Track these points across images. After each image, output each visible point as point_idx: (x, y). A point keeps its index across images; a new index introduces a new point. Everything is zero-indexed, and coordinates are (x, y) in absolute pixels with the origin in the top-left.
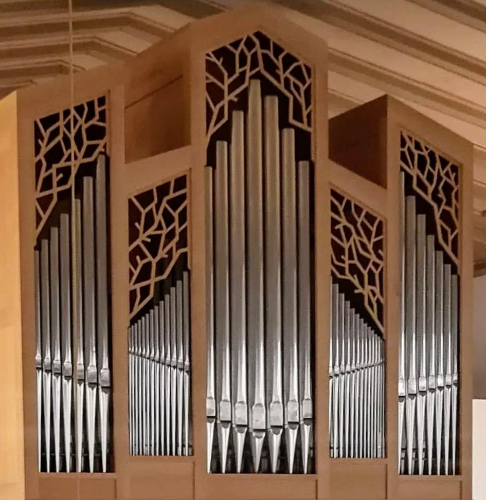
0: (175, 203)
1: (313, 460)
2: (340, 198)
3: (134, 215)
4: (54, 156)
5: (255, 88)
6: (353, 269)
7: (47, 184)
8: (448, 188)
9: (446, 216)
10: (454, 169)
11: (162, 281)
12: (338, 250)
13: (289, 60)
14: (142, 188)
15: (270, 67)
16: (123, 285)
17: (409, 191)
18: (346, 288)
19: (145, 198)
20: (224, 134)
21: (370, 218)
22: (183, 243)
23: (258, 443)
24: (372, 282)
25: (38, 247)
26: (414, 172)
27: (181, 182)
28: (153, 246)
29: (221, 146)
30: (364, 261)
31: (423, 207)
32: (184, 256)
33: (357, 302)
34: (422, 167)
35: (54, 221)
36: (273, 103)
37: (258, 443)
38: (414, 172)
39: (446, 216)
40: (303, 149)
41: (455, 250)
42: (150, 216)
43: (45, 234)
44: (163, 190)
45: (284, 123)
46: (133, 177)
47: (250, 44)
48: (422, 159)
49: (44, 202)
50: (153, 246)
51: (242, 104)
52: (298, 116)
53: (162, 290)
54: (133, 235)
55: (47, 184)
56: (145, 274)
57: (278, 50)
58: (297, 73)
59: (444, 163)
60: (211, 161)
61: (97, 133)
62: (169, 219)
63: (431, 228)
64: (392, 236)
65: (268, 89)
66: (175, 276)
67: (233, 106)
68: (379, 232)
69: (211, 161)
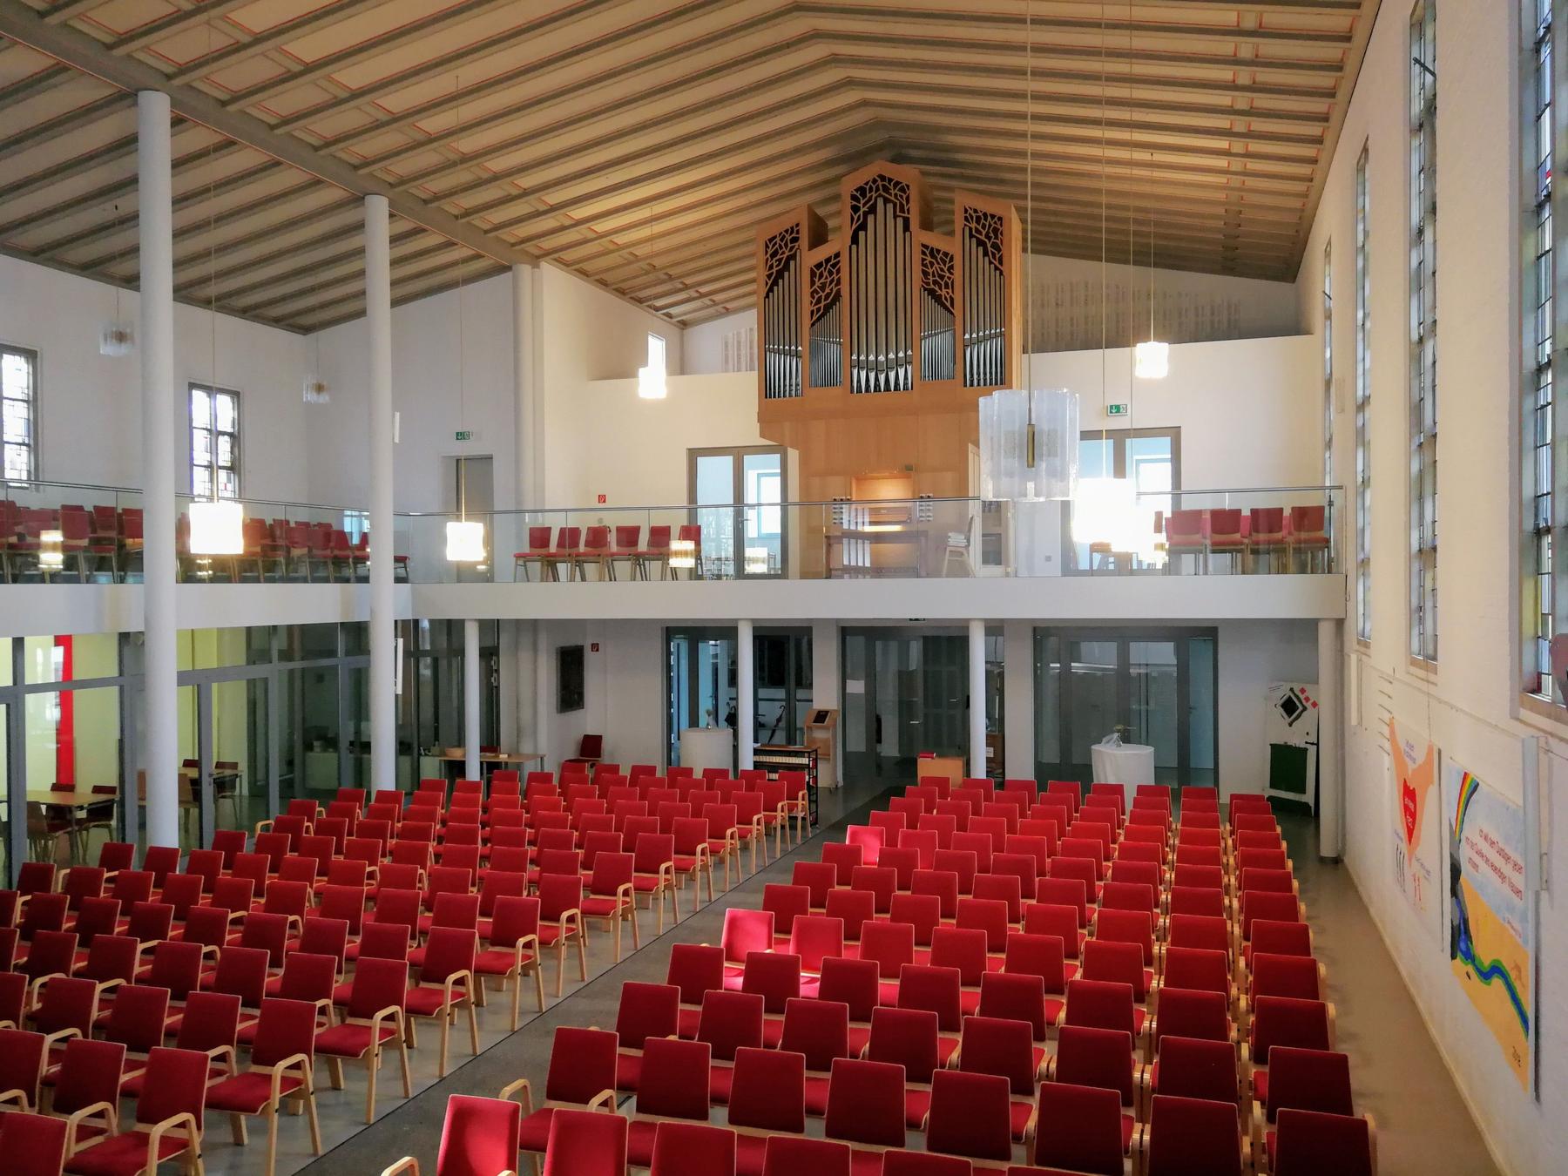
0: (834, 266)
1: (905, 384)
2: (926, 247)
3: (813, 274)
4: (774, 255)
5: (880, 202)
6: (935, 282)
7: (771, 267)
8: (996, 231)
9: (995, 246)
10: (1000, 219)
11: (826, 306)
12: (925, 274)
13: (897, 183)
14: (816, 261)
15: (886, 189)
16: (807, 305)
17: (971, 236)
18: (932, 293)
19: (819, 266)
20: (863, 227)
21: (946, 254)
22: (838, 283)
23: (882, 378)
24: (947, 286)
25: (767, 296)
26: (973, 225)
27: (837, 255)
28: (823, 288)
29: (862, 234)
30: (942, 277)
31: (980, 243)
32: (838, 292)
33: (937, 299)
34: (978, 221)
35: (775, 283)
36: (890, 206)
37: (882, 378)
38: (973, 225)
39: (995, 246)
40: (906, 228)
41: (1001, 262)
42: (821, 276)
43: (771, 290)
44: (828, 260)
45: (895, 217)
46: (810, 258)
47: (875, 181)
48: (978, 219)
49: (769, 276)
50: (823, 288)
51: (873, 210)
52: (902, 210)
53: (828, 308)
54: (813, 283)
55: (771, 267)
56: (819, 301)
57: (890, 180)
58: (903, 190)
59: (993, 216)
60: (855, 240)
61: (795, 240)
62: (831, 273)
63: (986, 254)
64: (957, 263)
65: (886, 201)
66: (834, 302)
67: (866, 214)
68: (952, 259)
69: (855, 240)
